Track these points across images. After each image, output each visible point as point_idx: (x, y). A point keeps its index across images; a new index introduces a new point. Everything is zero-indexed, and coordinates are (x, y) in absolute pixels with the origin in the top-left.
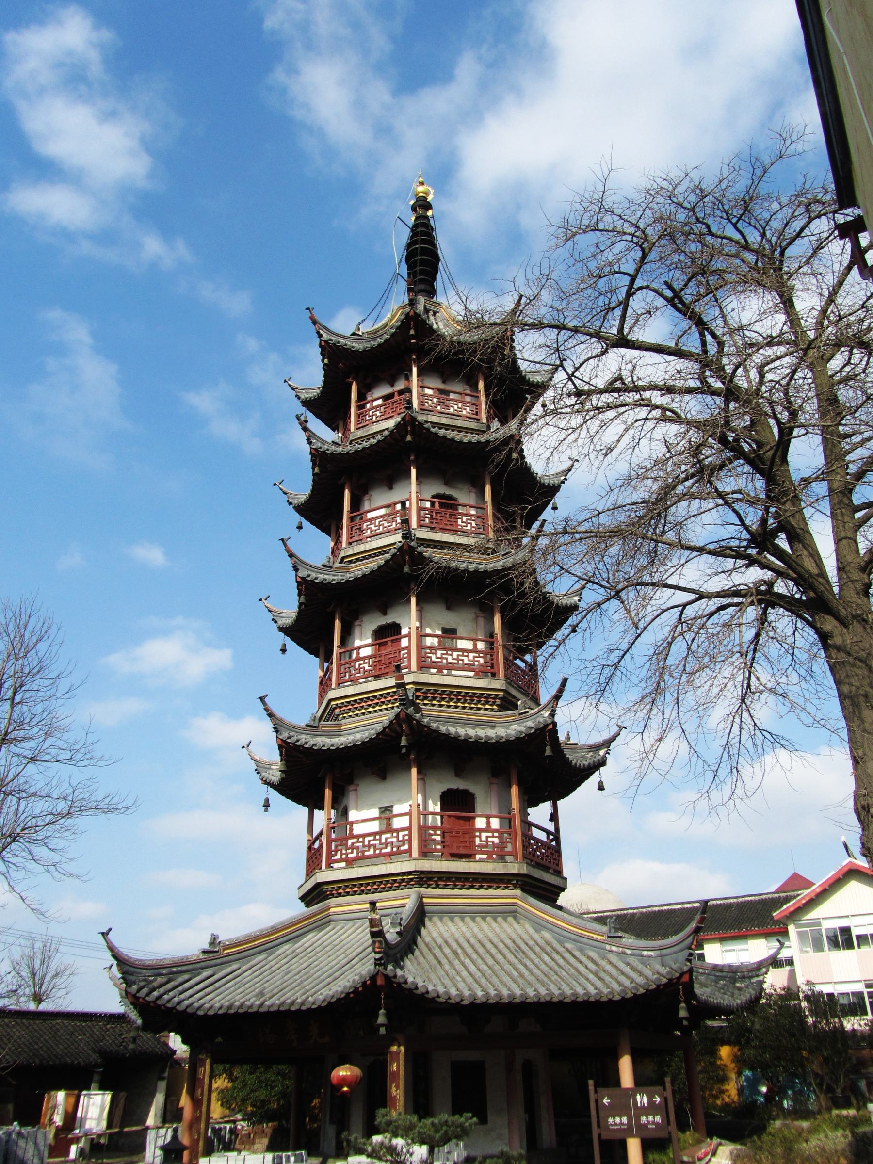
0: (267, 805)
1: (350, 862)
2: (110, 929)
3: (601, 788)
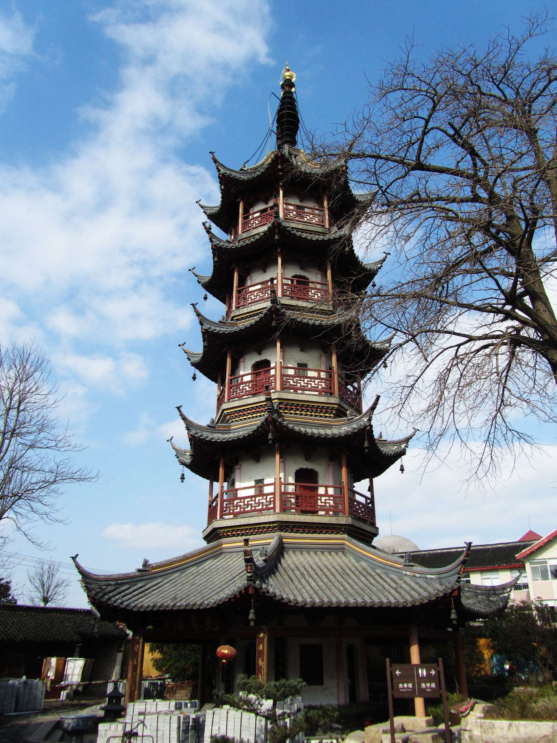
0: (183, 478)
1: (236, 515)
2: (77, 555)
3: (402, 469)
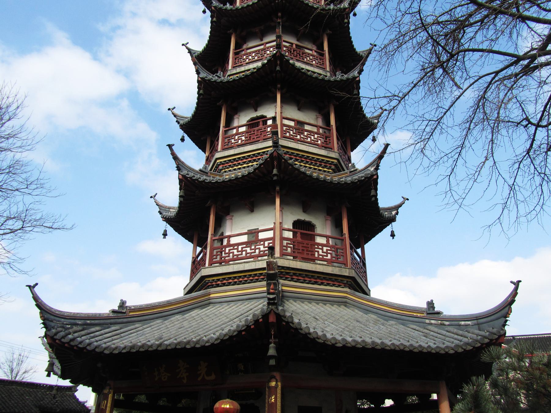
0: (165, 235)
1: (227, 262)
2: (37, 284)
3: (393, 235)
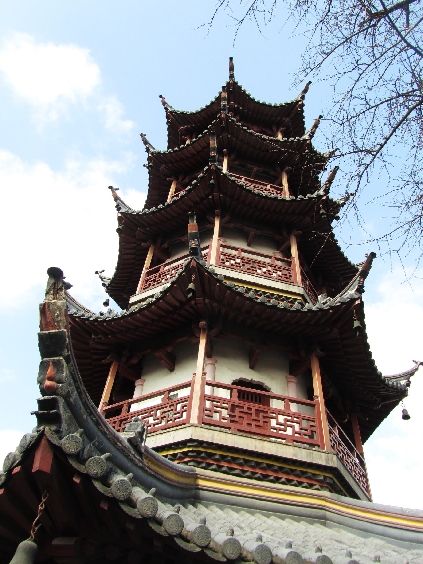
3: (406, 417)
